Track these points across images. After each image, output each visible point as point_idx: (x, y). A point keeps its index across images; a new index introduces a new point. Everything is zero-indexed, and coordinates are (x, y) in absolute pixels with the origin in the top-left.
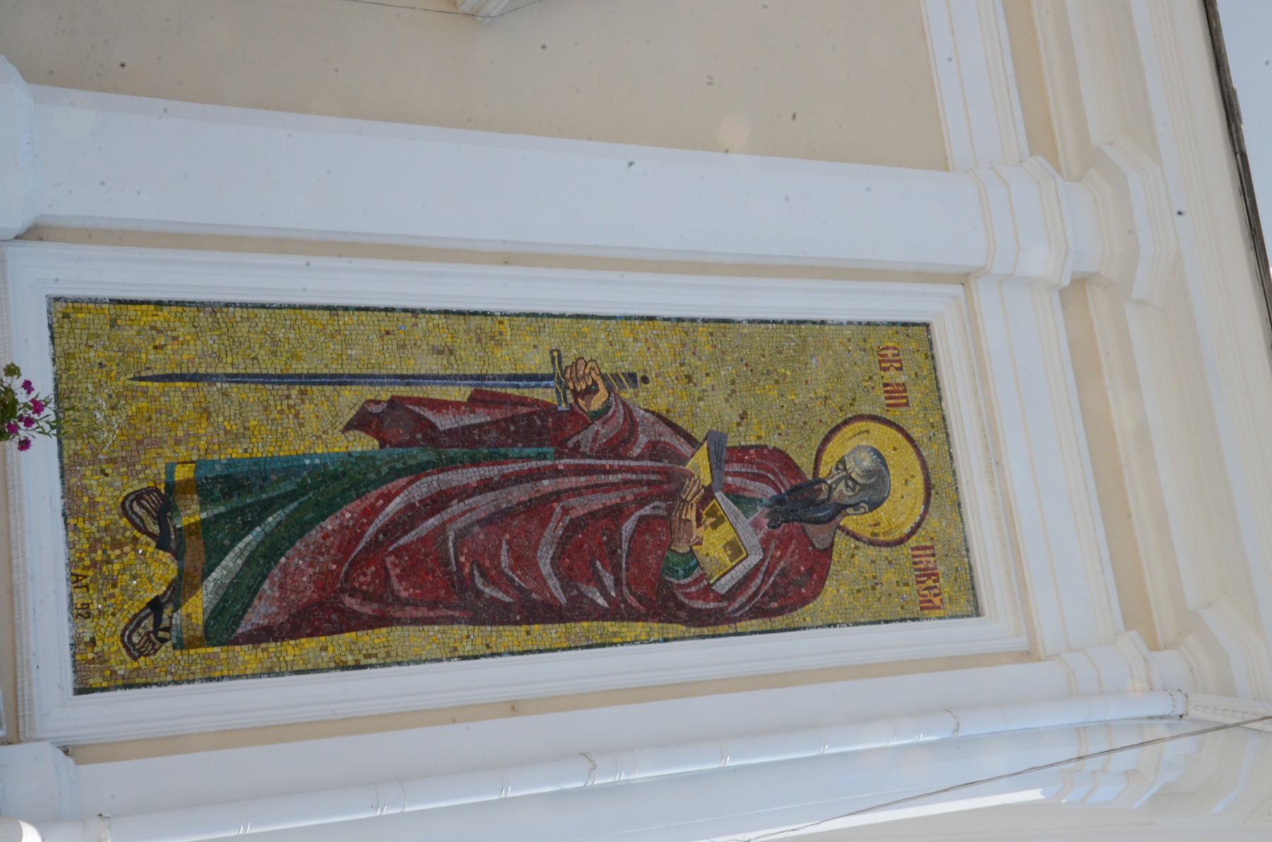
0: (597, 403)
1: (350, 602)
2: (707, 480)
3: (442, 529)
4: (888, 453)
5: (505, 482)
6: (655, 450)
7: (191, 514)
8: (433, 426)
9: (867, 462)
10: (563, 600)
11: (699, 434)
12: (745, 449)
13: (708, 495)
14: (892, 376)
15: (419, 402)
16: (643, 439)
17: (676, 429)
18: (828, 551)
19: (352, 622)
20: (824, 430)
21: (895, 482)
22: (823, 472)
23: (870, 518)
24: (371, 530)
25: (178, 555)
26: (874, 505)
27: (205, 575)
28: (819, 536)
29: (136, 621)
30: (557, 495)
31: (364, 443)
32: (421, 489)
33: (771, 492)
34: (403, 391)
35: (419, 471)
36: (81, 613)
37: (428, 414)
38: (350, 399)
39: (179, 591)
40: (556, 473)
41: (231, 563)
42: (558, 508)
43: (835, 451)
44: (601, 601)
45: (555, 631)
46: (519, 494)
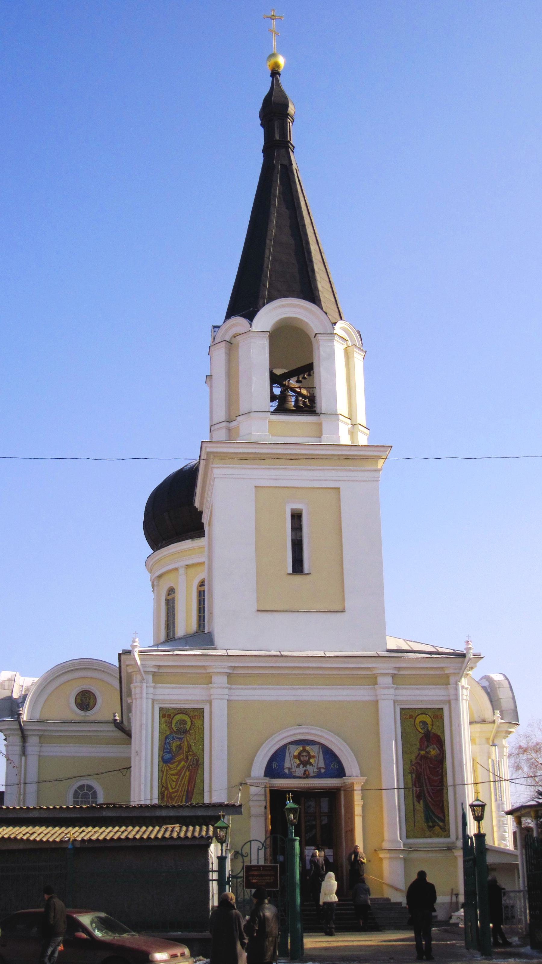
0: (415, 768)
1: (441, 805)
2: (424, 752)
3: (433, 793)
4: (420, 720)
5: (426, 783)
6: (421, 759)
7: (431, 824)
8: (419, 792)
9: (421, 724)
10: (440, 776)
11: (418, 752)
12: (420, 745)
13: (426, 752)
14: (408, 717)
15: (416, 794)
16: (419, 762)
17: (418, 756)
18: (434, 733)
19: (443, 805)
20: (417, 731)
21: (424, 720)
22: (423, 732)
23: (429, 725)
24: (432, 802)
25: (435, 825)
26: (427, 724)
27: (437, 822)
28: (431, 735)
29: (442, 831)
30: (427, 775)
31: (421, 802)
32: (427, 795)
33: (426, 742)
34: (415, 795)
35: (425, 795)
36: (441, 837)
37: (418, 793)
38: (416, 803)
39: (439, 826)
40: (424, 775)
41: (436, 820)
42: (429, 776)
43: (420, 730)
44: (441, 771)
45: (444, 778)
46: (427, 781)
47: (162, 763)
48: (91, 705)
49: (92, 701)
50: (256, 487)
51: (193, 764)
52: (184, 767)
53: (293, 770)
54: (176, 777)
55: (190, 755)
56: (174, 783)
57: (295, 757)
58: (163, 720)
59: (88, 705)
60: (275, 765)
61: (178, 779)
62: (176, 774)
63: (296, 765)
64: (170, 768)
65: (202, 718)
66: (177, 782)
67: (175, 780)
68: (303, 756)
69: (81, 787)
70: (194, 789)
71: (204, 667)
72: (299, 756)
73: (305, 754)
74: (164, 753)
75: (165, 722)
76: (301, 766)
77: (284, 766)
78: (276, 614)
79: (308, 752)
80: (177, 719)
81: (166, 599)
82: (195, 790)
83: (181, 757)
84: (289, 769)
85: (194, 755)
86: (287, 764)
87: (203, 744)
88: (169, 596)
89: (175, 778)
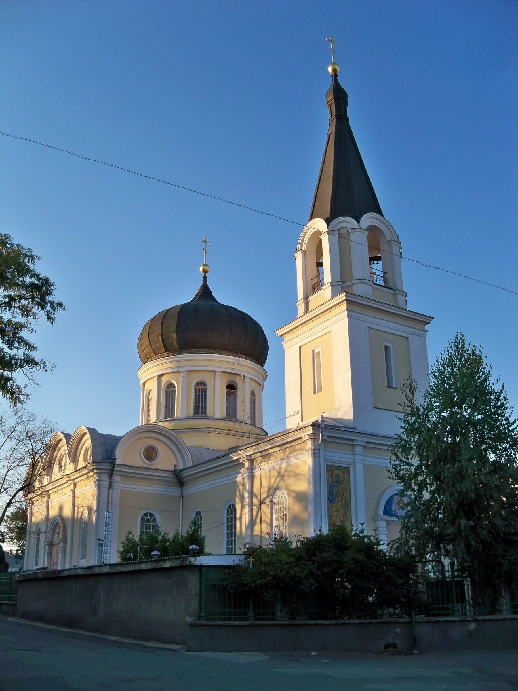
47: (328, 502)
48: (153, 458)
49: (154, 454)
50: (369, 327)
51: (345, 504)
52: (340, 506)
53: (397, 512)
54: (337, 512)
55: (344, 498)
56: (336, 516)
57: (397, 504)
58: (328, 473)
59: (152, 457)
60: (387, 509)
61: (337, 514)
62: (337, 510)
63: (398, 509)
64: (333, 506)
65: (348, 474)
66: (337, 515)
67: (336, 514)
68: (401, 503)
69: (146, 515)
70: (346, 521)
71: (352, 440)
72: (398, 504)
73: (401, 502)
74: (329, 495)
75: (329, 475)
76: (400, 509)
77: (392, 509)
78: (383, 410)
79: (402, 501)
80: (336, 473)
81: (165, 391)
82: (347, 522)
83: (339, 499)
84: (395, 511)
85: (346, 498)
86: (393, 509)
87: (350, 492)
88: (168, 389)
89: (336, 513)
